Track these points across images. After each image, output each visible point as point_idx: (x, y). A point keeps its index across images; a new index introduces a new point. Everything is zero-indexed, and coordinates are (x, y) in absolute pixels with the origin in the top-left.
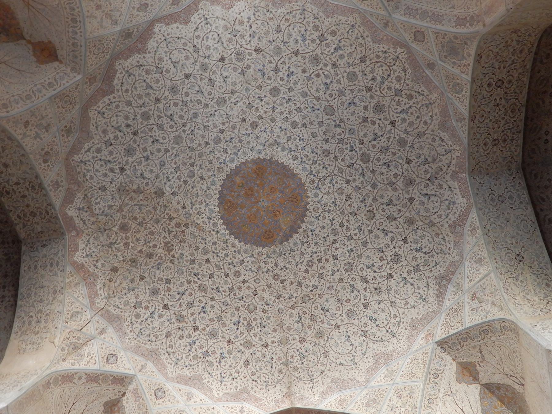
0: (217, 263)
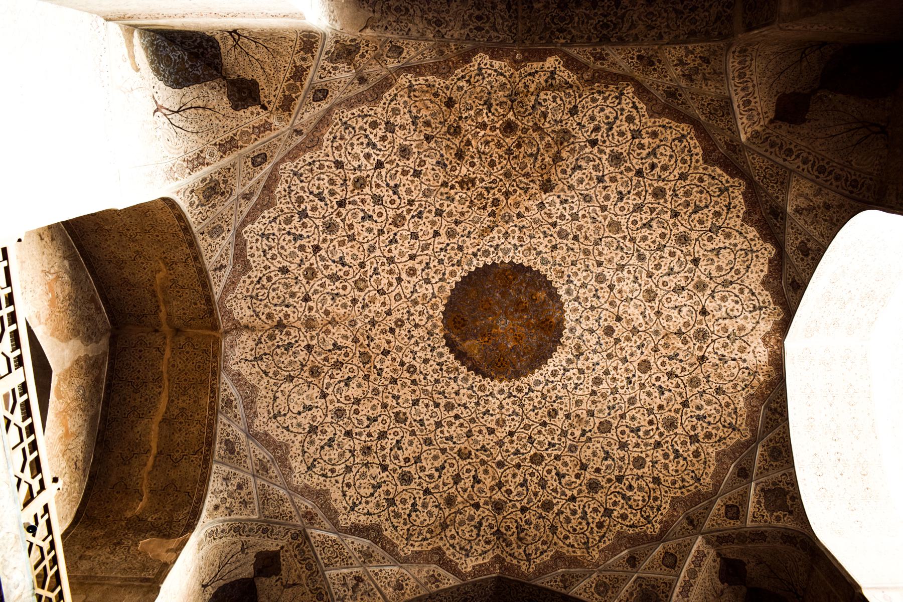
0: (431, 247)
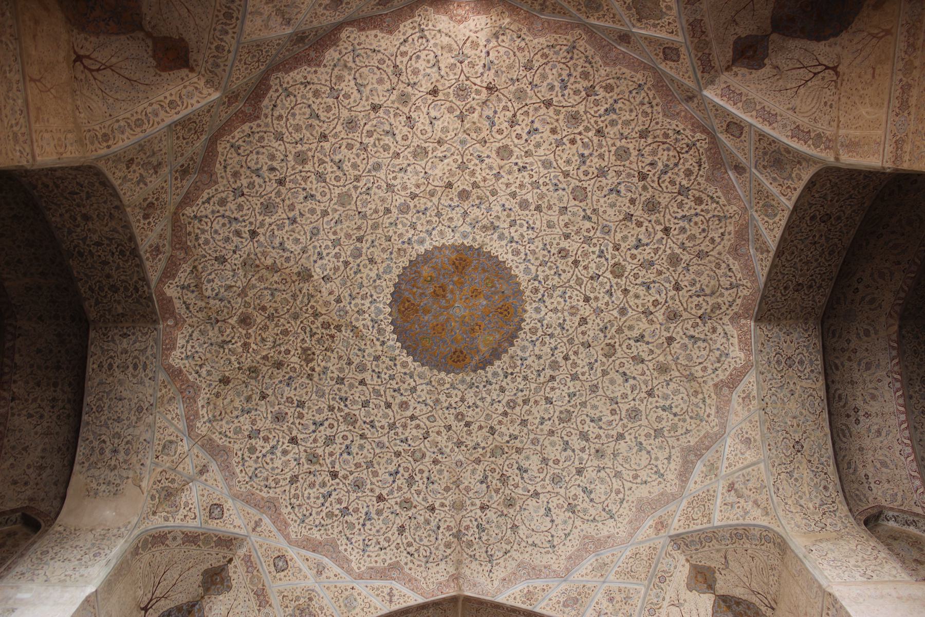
0: (377, 387)
